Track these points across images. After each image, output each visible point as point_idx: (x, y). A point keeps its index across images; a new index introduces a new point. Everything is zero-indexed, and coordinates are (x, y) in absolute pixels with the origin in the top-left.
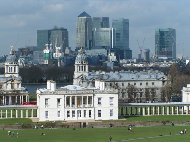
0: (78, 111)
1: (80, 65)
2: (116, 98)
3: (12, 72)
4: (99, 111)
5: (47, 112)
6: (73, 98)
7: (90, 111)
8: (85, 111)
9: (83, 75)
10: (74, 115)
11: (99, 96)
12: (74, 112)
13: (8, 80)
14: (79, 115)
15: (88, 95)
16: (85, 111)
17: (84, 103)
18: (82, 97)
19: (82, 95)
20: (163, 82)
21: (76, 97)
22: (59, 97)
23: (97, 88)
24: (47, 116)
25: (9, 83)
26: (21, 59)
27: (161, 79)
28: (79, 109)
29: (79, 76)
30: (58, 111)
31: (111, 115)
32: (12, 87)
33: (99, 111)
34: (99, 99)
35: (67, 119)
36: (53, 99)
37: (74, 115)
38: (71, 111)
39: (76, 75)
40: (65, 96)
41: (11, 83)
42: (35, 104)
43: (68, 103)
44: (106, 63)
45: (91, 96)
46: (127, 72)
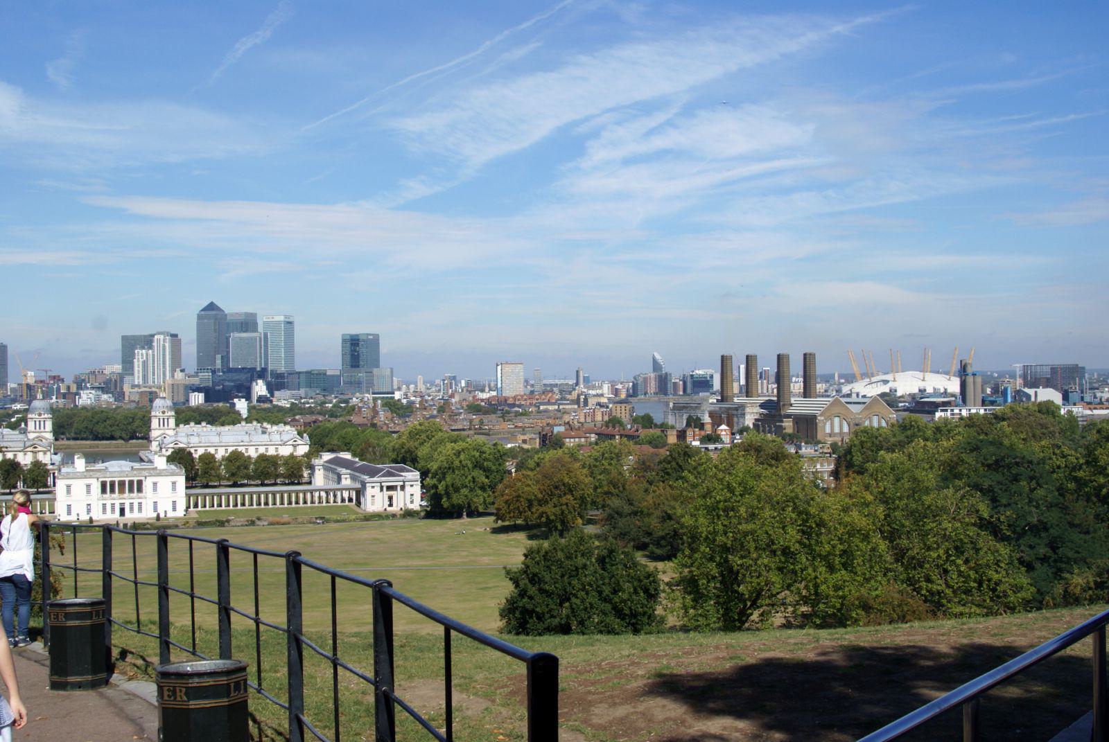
2: (181, 481)
3: (40, 428)
5: (69, 506)
6: (112, 484)
7: (140, 504)
8: (132, 504)
12: (113, 505)
14: (122, 512)
15: (135, 479)
16: (132, 504)
17: (131, 491)
19: (127, 479)
20: (295, 446)
24: (69, 513)
26: (88, 391)
27: (291, 442)
28: (122, 501)
31: (174, 509)
32: (35, 457)
34: (155, 484)
36: (78, 486)
39: (154, 434)
43: (104, 491)
44: (234, 404)
46: (250, 425)
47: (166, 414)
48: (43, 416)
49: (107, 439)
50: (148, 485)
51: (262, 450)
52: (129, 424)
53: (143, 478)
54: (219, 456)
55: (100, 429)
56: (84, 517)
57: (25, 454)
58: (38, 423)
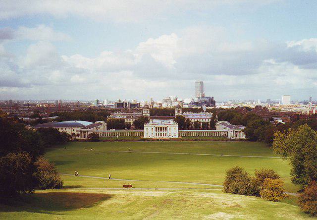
2: (177, 128)
6: (159, 128)
14: (161, 136)
17: (164, 130)
39: (176, 115)
43: (156, 130)
50: (168, 129)
51: (204, 121)
54: (193, 121)
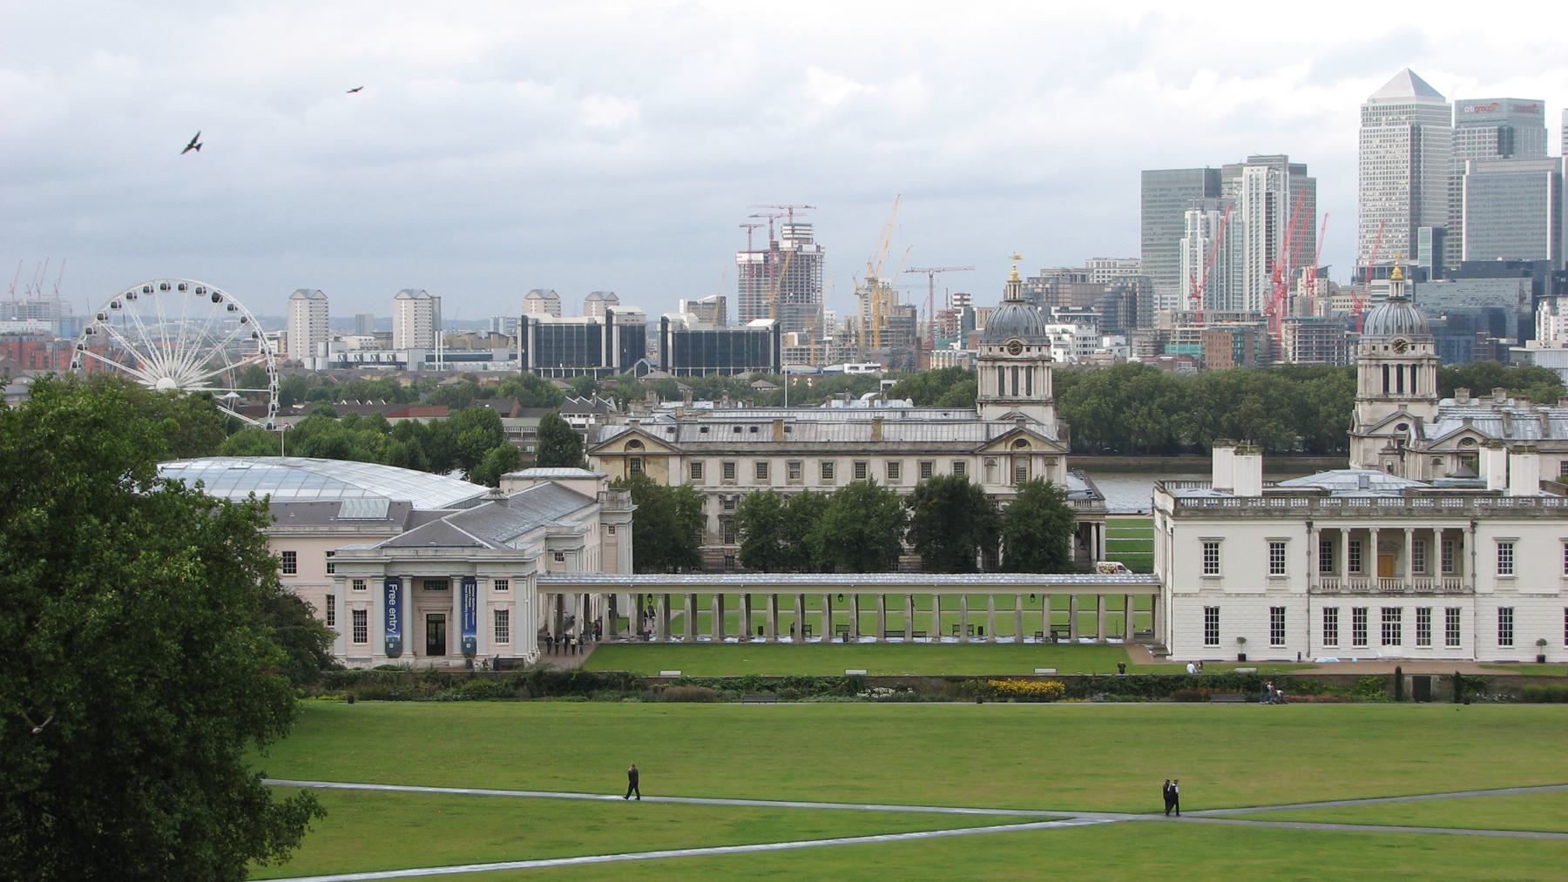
0: (1384, 610)
1: (1390, 363)
3: (1015, 393)
4: (1506, 615)
5: (1212, 615)
7: (1453, 615)
8: (1423, 615)
9: (1403, 416)
10: (1360, 636)
11: (1505, 529)
12: (1360, 615)
13: (995, 433)
14: (1391, 635)
15: (1438, 525)
16: (1423, 615)
17: (1421, 566)
18: (1409, 537)
19: (1409, 525)
21: (1374, 537)
22: (1278, 529)
23: (1489, 489)
24: (1212, 636)
25: (1002, 454)
28: (1392, 602)
29: (1380, 417)
30: (1272, 610)
32: (1018, 475)
33: (1506, 615)
34: (1506, 550)
35: (1323, 655)
36: (1245, 545)
37: (1360, 636)
38: (1345, 607)
40: (1310, 525)
41: (1012, 456)
42: (1150, 570)
45: (1458, 533)
47: (1409, 352)
48: (1024, 354)
49: (1154, 451)
52: (1223, 407)
53: (1464, 525)
55: (1136, 418)
56: (1262, 651)
57: (990, 465)
58: (1008, 375)
